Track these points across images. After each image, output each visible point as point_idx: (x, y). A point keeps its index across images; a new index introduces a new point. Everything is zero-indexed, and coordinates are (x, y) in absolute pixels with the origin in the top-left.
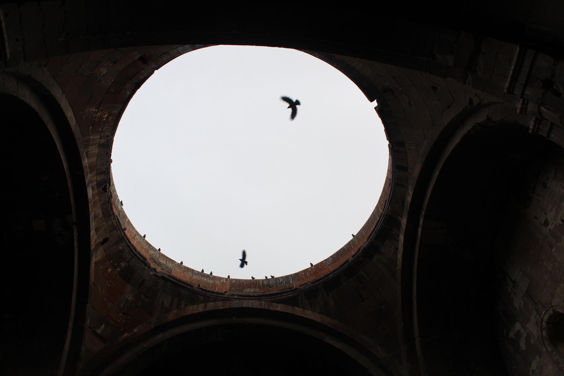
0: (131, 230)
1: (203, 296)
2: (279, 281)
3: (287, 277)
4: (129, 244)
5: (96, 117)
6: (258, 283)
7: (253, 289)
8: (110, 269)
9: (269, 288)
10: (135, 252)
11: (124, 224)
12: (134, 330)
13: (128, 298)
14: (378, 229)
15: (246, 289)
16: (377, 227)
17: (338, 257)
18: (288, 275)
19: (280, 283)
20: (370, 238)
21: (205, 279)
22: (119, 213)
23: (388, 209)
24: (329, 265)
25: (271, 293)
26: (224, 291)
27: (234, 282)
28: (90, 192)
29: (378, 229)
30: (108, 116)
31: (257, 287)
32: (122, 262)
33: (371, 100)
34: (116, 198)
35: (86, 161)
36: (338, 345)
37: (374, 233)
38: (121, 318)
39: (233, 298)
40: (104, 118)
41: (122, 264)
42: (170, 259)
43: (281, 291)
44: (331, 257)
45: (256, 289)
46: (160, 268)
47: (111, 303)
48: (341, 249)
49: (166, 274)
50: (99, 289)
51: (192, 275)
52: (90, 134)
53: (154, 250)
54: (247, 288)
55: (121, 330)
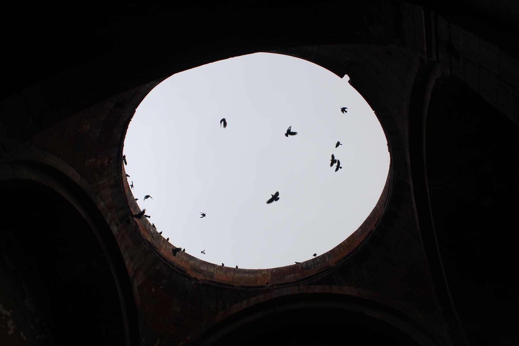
0: (168, 247)
2: (317, 261)
4: (165, 262)
5: (97, 166)
6: (298, 268)
7: (292, 275)
9: (308, 270)
10: (172, 268)
11: (160, 244)
15: (287, 276)
16: (389, 193)
17: (366, 227)
18: (324, 254)
20: (386, 205)
21: (247, 275)
22: (153, 236)
23: (394, 174)
24: (359, 236)
25: (310, 275)
26: (266, 282)
27: (274, 271)
28: (114, 229)
30: (108, 160)
31: (297, 271)
33: (342, 76)
34: (147, 223)
35: (102, 204)
37: (388, 199)
39: (274, 289)
40: (105, 164)
41: (163, 282)
42: (211, 263)
43: (320, 271)
44: (360, 227)
45: (296, 274)
46: (202, 275)
48: (367, 218)
49: (207, 280)
51: (234, 274)
52: (97, 181)
53: (193, 260)
54: (287, 275)
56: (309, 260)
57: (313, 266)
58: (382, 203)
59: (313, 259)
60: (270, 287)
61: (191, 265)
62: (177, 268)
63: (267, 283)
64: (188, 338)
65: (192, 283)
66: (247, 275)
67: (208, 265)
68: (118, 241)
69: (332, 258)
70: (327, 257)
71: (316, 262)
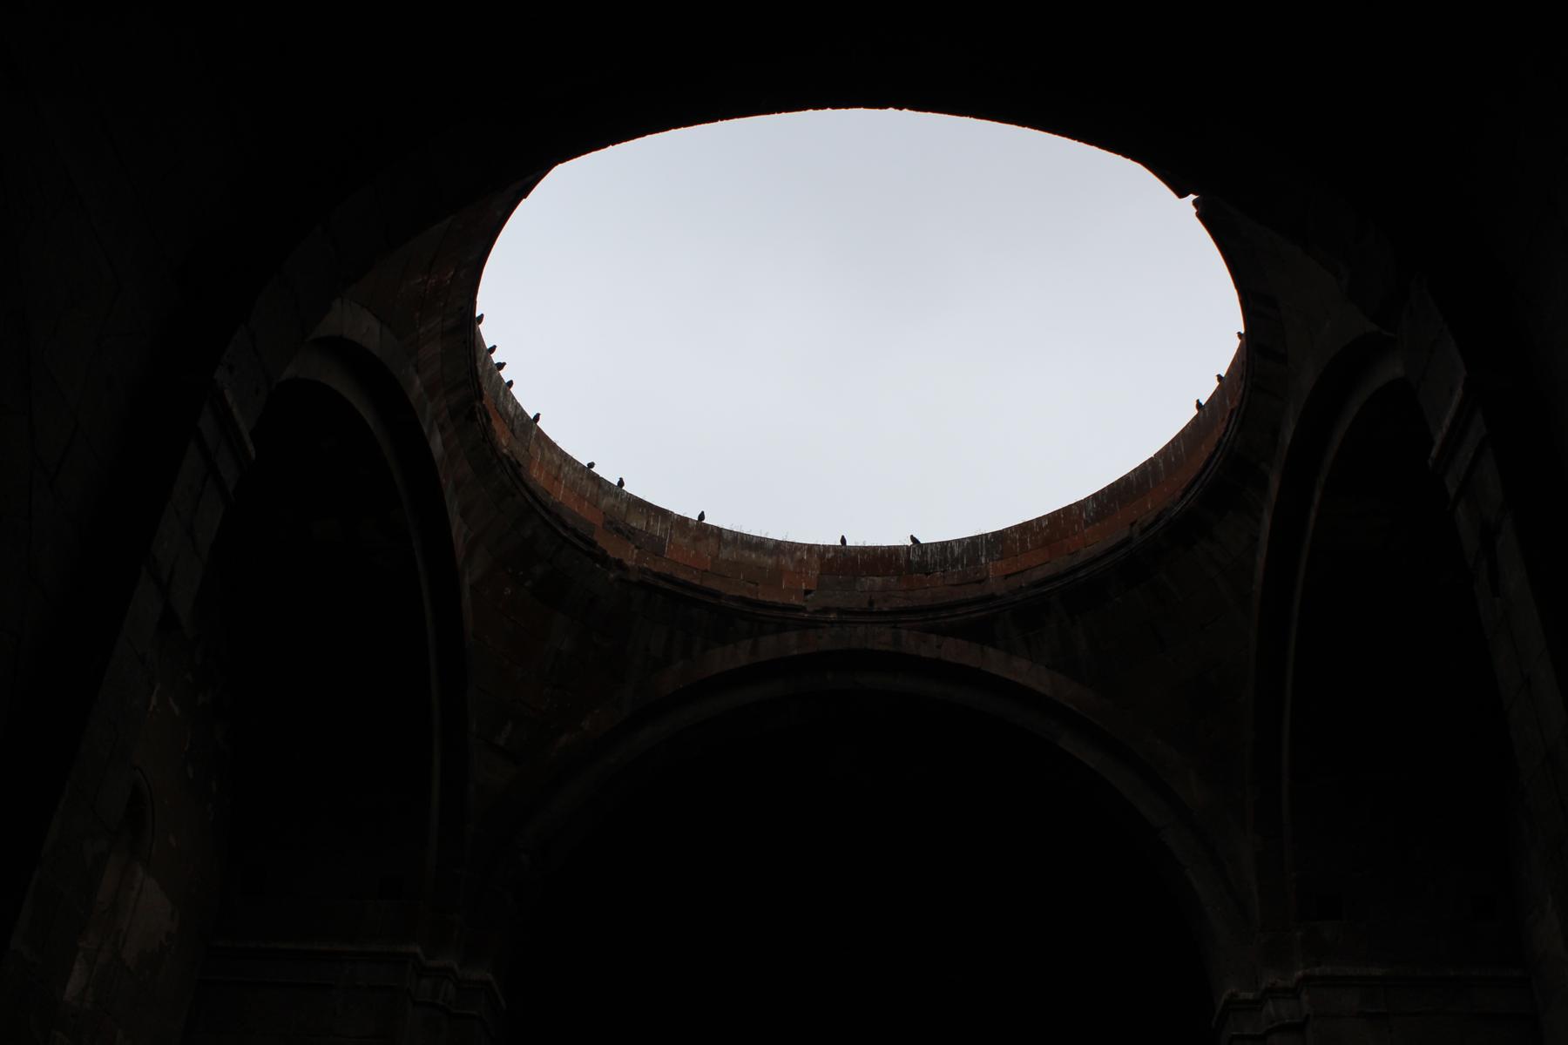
0: (547, 455)
3: (974, 541)
4: (547, 517)
5: (426, 290)
6: (896, 559)
7: (878, 580)
8: (507, 589)
10: (565, 534)
11: (528, 451)
14: (1208, 480)
15: (863, 579)
17: (1112, 505)
18: (977, 537)
19: (957, 561)
20: (1189, 496)
22: (513, 424)
26: (804, 588)
28: (437, 444)
29: (1208, 480)
33: (1181, 194)
34: (500, 388)
35: (418, 382)
37: (1196, 487)
39: (827, 622)
44: (1095, 496)
46: (633, 546)
53: (611, 496)
54: (863, 576)
56: (931, 544)
57: (940, 566)
58: (1173, 459)
59: (943, 542)
60: (816, 612)
61: (604, 513)
63: (807, 592)
65: (612, 576)
66: (754, 556)
67: (648, 511)
68: (441, 476)
69: (997, 560)
70: (984, 550)
71: (949, 556)
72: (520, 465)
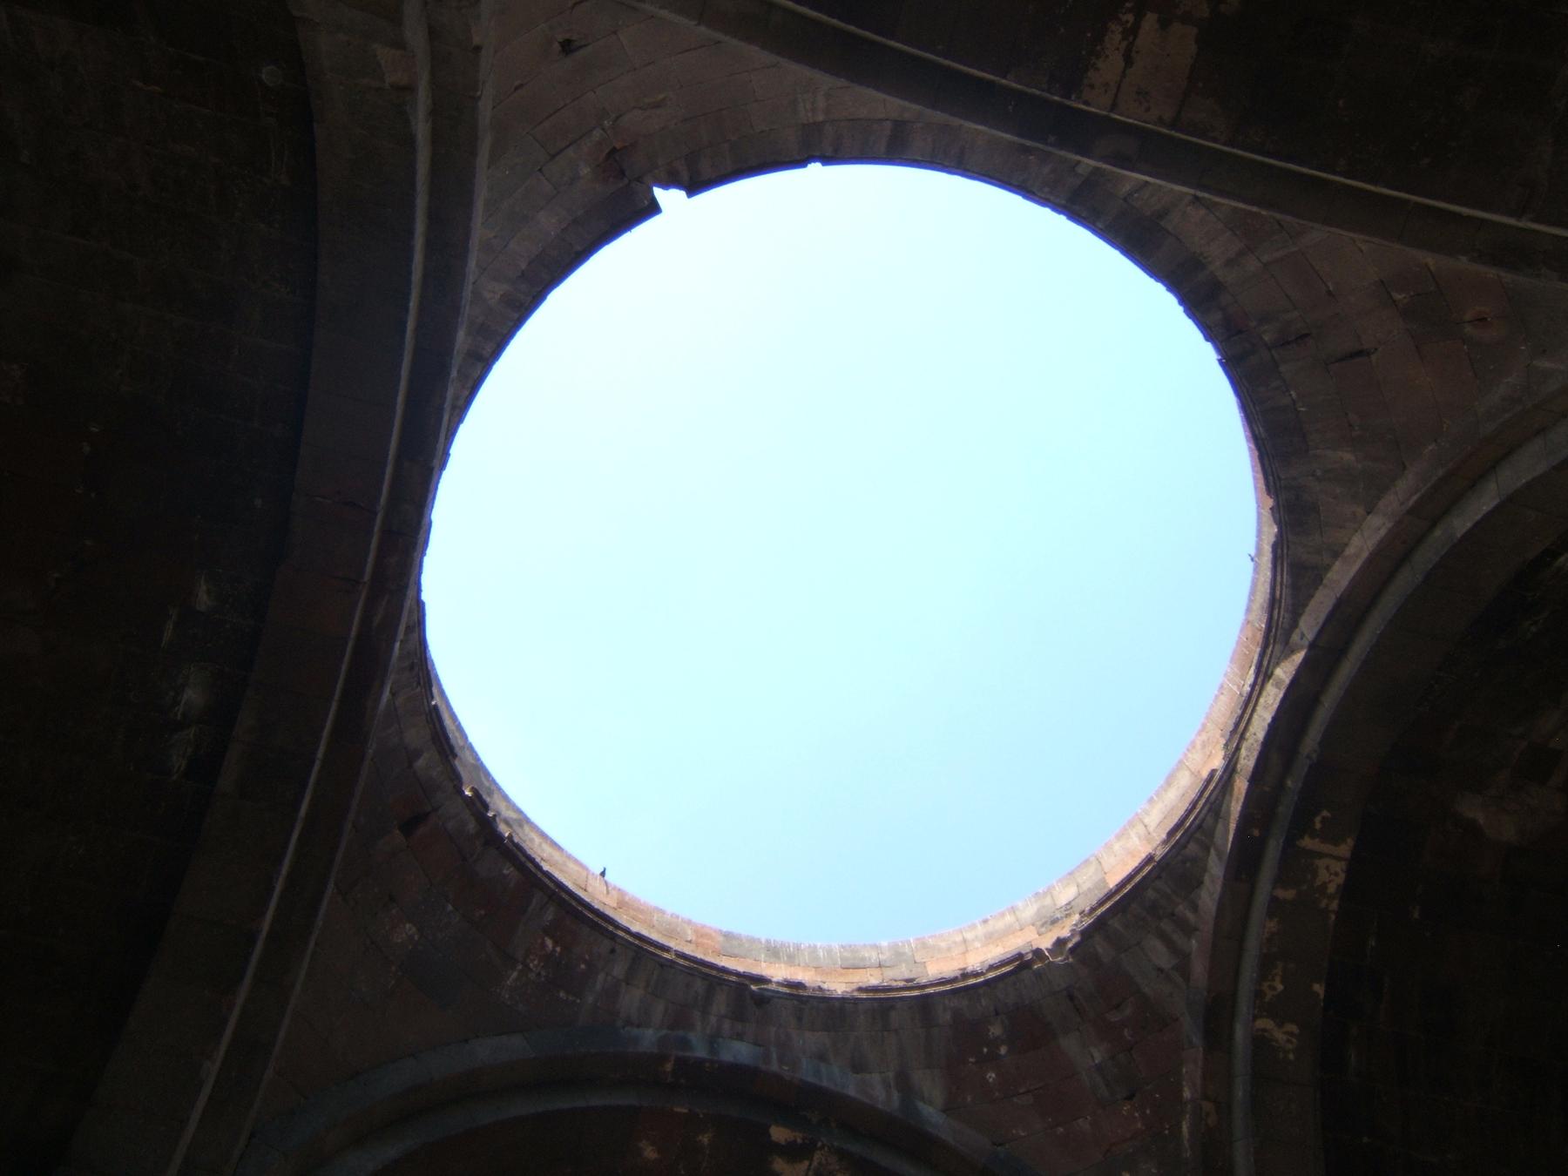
1: (1188, 842)
5: (539, 974)
8: (989, 1075)
12: (1185, 1095)
13: (1097, 1062)
30: (551, 937)
32: (989, 1030)
33: (653, 209)
36: (1484, 502)
38: (1137, 1115)
40: (554, 950)
41: (993, 1033)
47: (1080, 1121)
50: (1023, 1134)
52: (578, 1001)
55: (1167, 1132)
62: (992, 968)
64: (1187, 1094)
72: (907, 981)
